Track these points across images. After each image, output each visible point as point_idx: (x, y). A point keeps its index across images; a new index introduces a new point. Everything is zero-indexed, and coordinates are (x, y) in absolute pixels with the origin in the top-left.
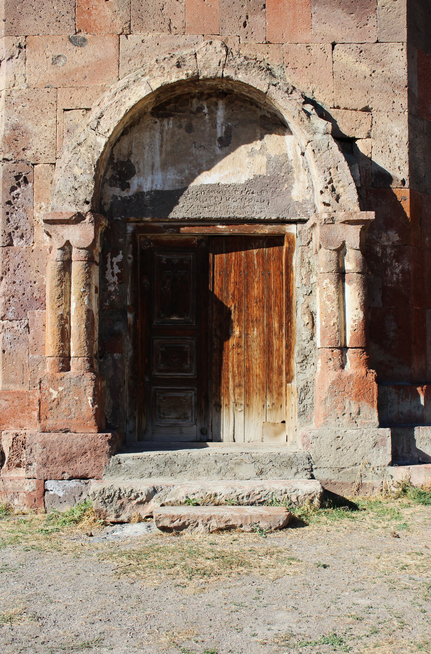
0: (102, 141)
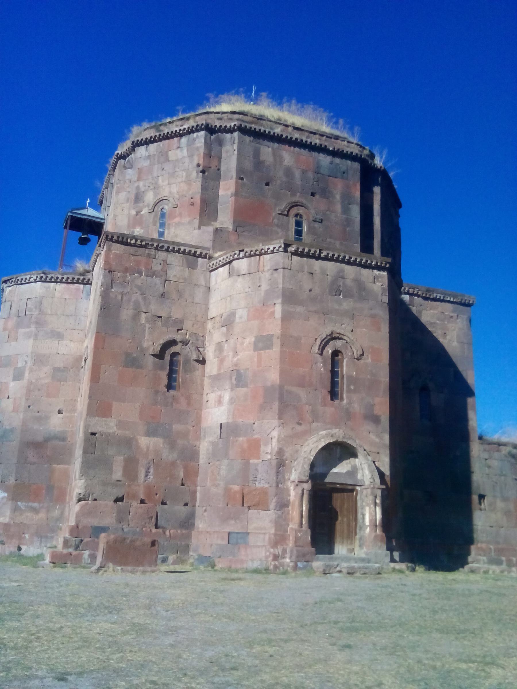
0: (312, 458)
